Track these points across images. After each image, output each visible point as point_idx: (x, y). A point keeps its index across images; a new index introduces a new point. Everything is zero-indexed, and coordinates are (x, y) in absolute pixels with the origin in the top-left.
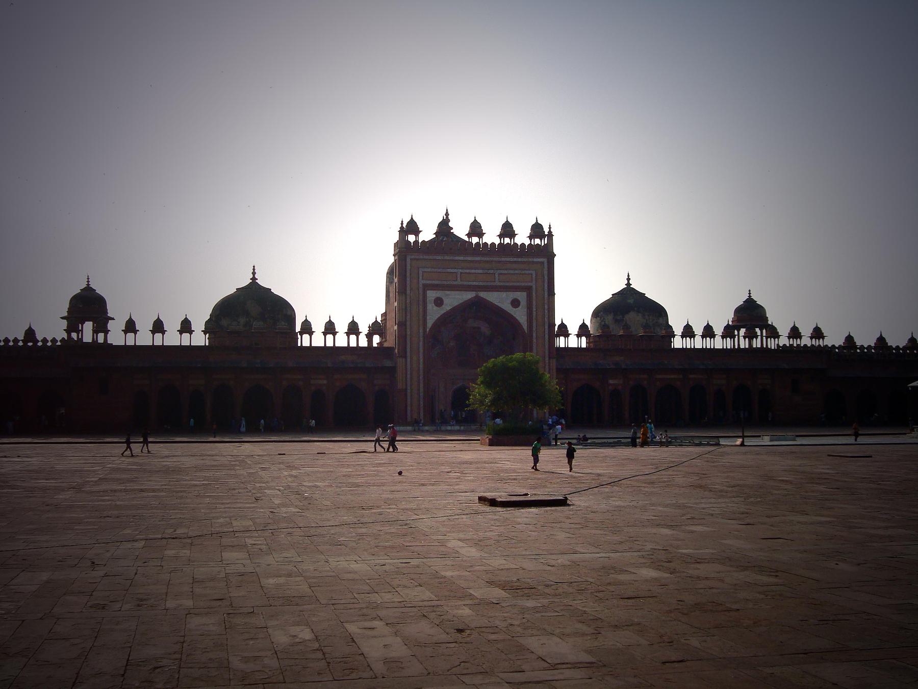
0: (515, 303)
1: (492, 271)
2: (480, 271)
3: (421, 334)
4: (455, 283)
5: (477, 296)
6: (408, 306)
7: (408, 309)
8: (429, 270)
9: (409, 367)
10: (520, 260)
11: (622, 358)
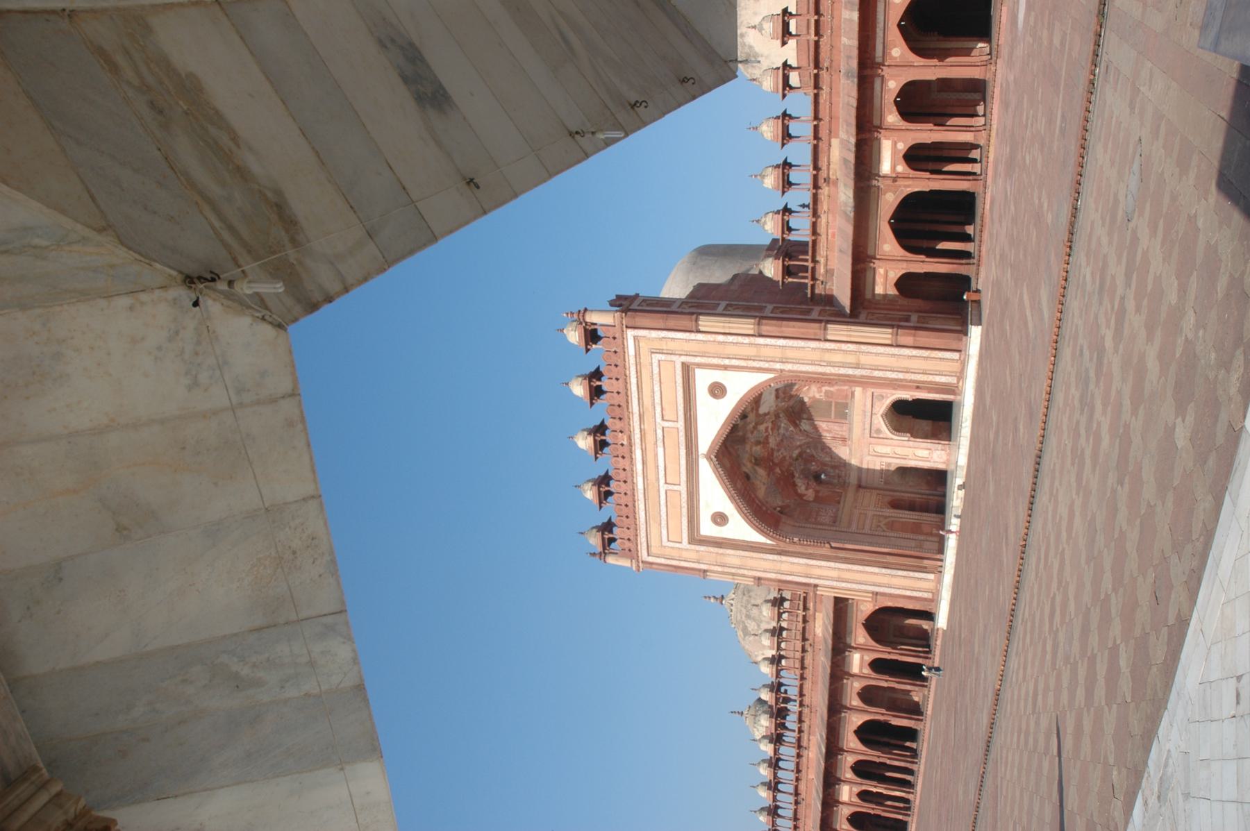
0: (717, 390)
1: (659, 432)
2: (660, 450)
3: (776, 557)
4: (684, 495)
5: (708, 457)
6: (726, 570)
7: (733, 571)
8: (664, 532)
9: (835, 584)
10: (633, 380)
11: (835, 142)
